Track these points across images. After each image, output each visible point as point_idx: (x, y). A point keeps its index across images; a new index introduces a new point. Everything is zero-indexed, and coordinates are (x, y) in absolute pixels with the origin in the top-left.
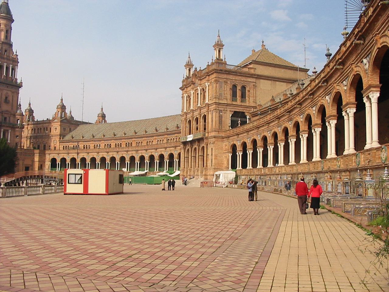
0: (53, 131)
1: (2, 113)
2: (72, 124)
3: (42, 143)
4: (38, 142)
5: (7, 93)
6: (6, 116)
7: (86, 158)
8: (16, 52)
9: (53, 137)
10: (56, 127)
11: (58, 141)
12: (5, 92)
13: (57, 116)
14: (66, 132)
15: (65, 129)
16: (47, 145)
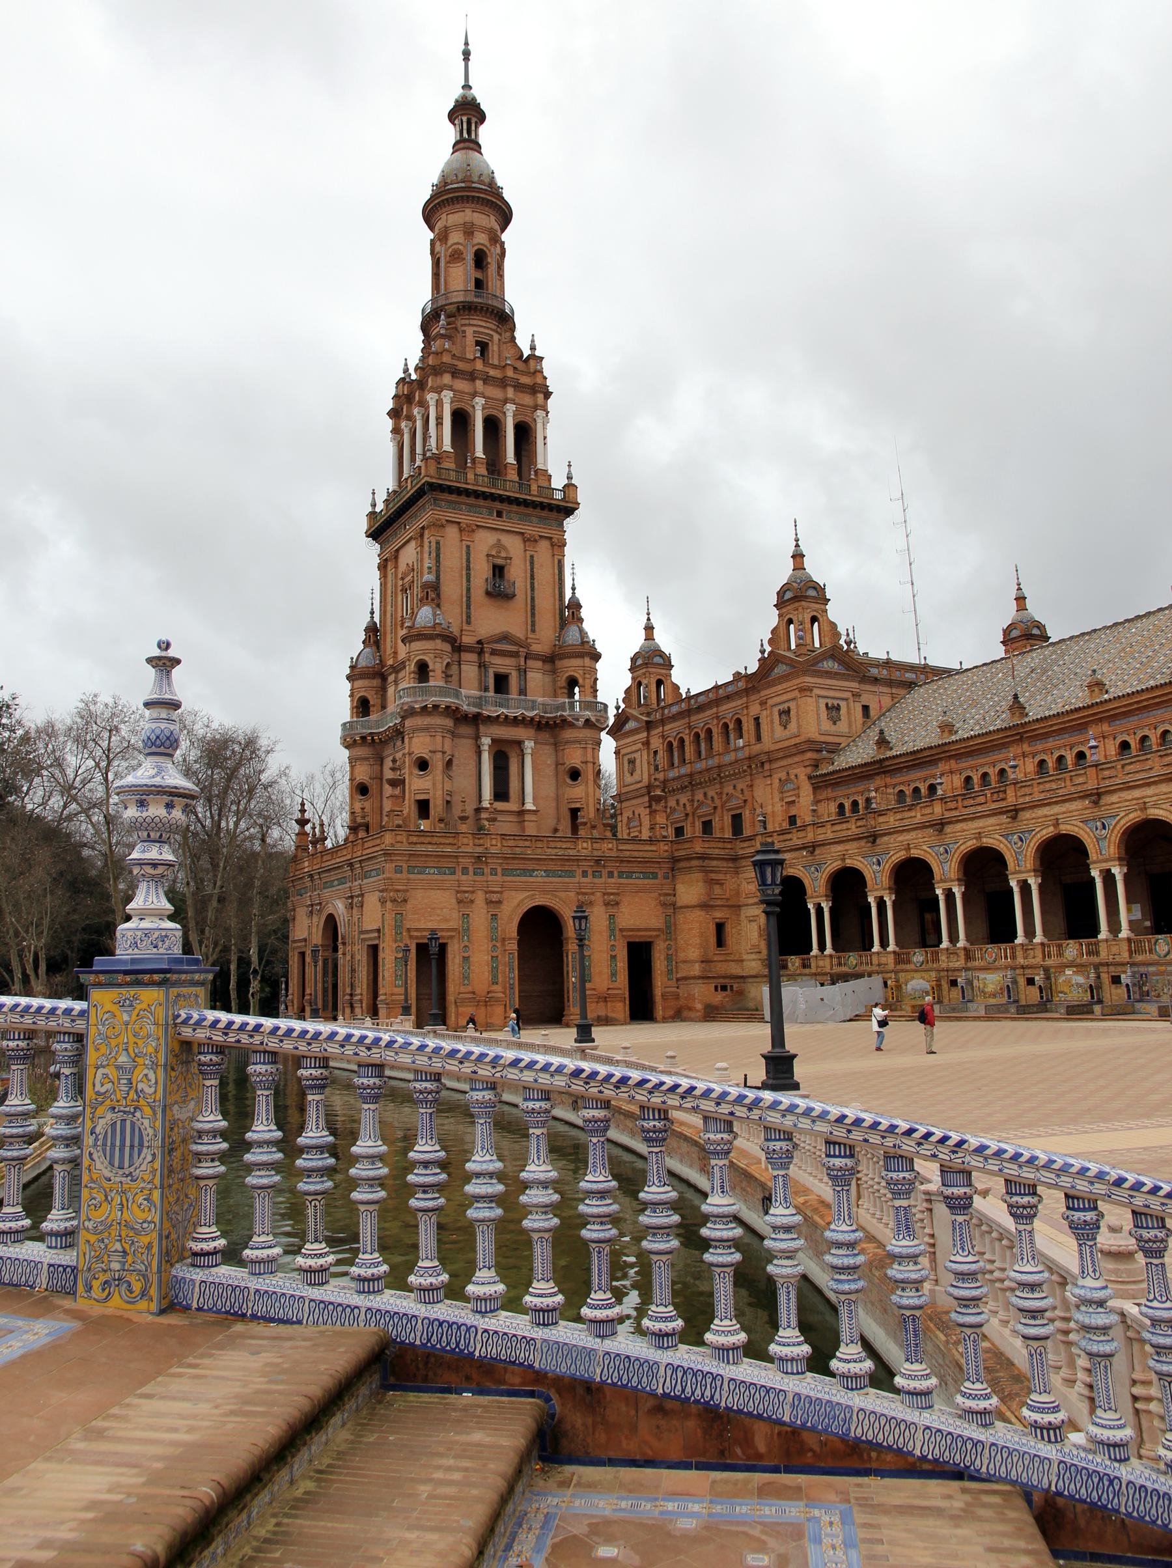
0: (773, 731)
1: (481, 653)
2: (876, 681)
3: (722, 806)
4: (701, 804)
5: (499, 545)
6: (501, 664)
7: (1002, 848)
8: (533, 348)
9: (775, 765)
10: (785, 706)
11: (803, 778)
12: (484, 541)
13: (783, 644)
14: (842, 726)
15: (838, 708)
16: (747, 815)
